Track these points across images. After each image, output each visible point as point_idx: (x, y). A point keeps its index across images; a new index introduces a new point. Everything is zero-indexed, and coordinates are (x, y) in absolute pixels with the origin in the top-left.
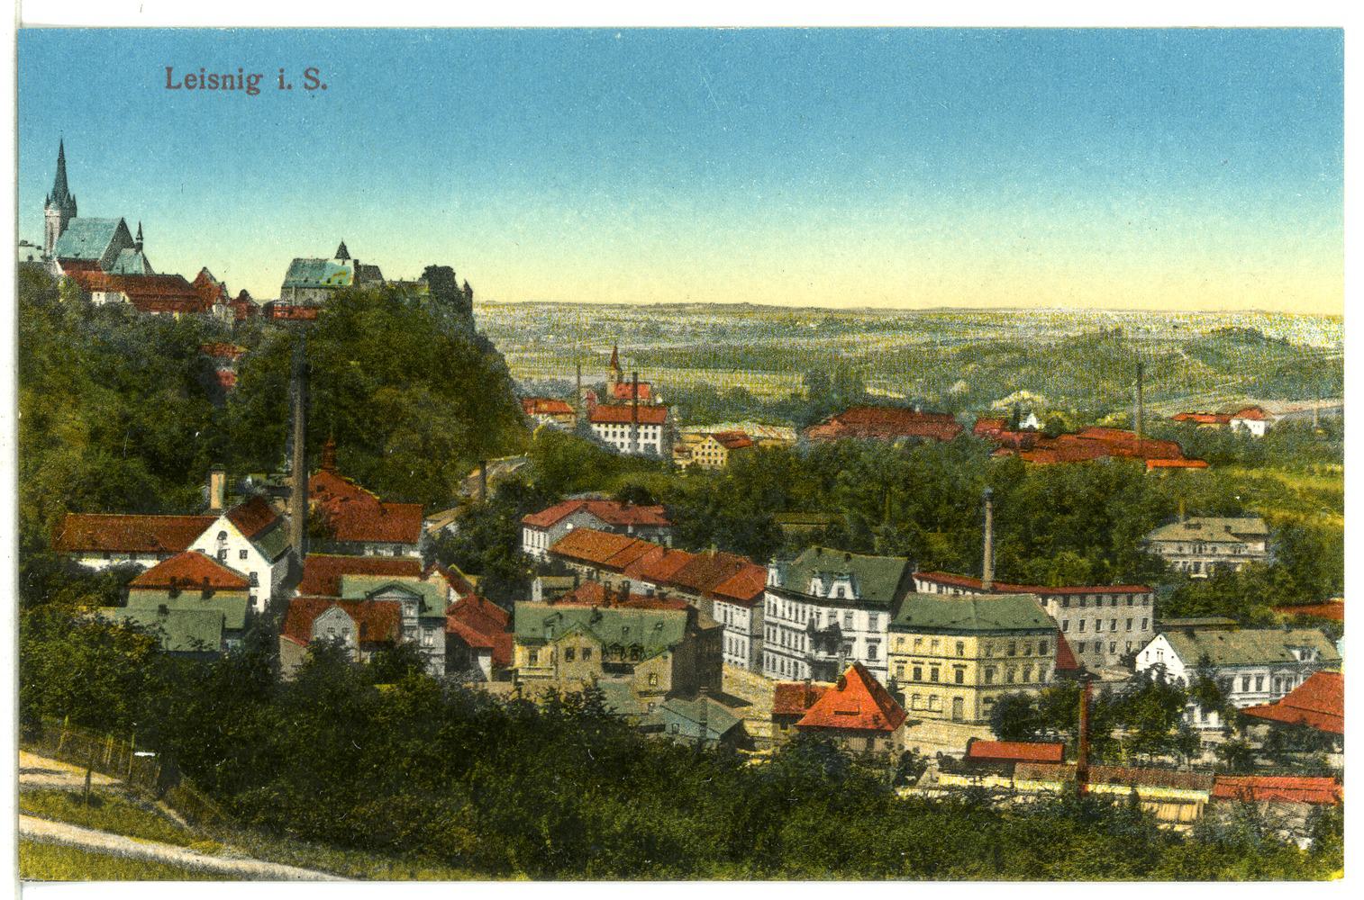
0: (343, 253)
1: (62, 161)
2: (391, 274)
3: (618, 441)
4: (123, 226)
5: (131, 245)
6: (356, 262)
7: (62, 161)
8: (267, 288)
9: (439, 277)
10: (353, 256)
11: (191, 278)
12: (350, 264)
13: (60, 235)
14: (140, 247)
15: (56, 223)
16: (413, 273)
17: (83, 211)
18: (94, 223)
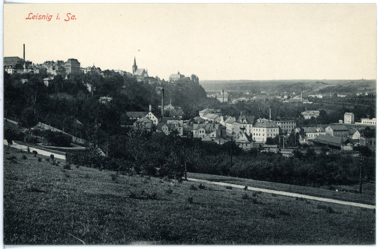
0: (179, 73)
1: (135, 61)
2: (186, 76)
3: (221, 100)
4: (144, 70)
5: (146, 73)
6: (181, 75)
7: (135, 61)
8: (167, 79)
9: (194, 76)
10: (180, 74)
11: (155, 77)
12: (180, 75)
13: (135, 71)
14: (147, 73)
15: (134, 70)
16: (190, 76)
17: (138, 68)
18: (140, 69)
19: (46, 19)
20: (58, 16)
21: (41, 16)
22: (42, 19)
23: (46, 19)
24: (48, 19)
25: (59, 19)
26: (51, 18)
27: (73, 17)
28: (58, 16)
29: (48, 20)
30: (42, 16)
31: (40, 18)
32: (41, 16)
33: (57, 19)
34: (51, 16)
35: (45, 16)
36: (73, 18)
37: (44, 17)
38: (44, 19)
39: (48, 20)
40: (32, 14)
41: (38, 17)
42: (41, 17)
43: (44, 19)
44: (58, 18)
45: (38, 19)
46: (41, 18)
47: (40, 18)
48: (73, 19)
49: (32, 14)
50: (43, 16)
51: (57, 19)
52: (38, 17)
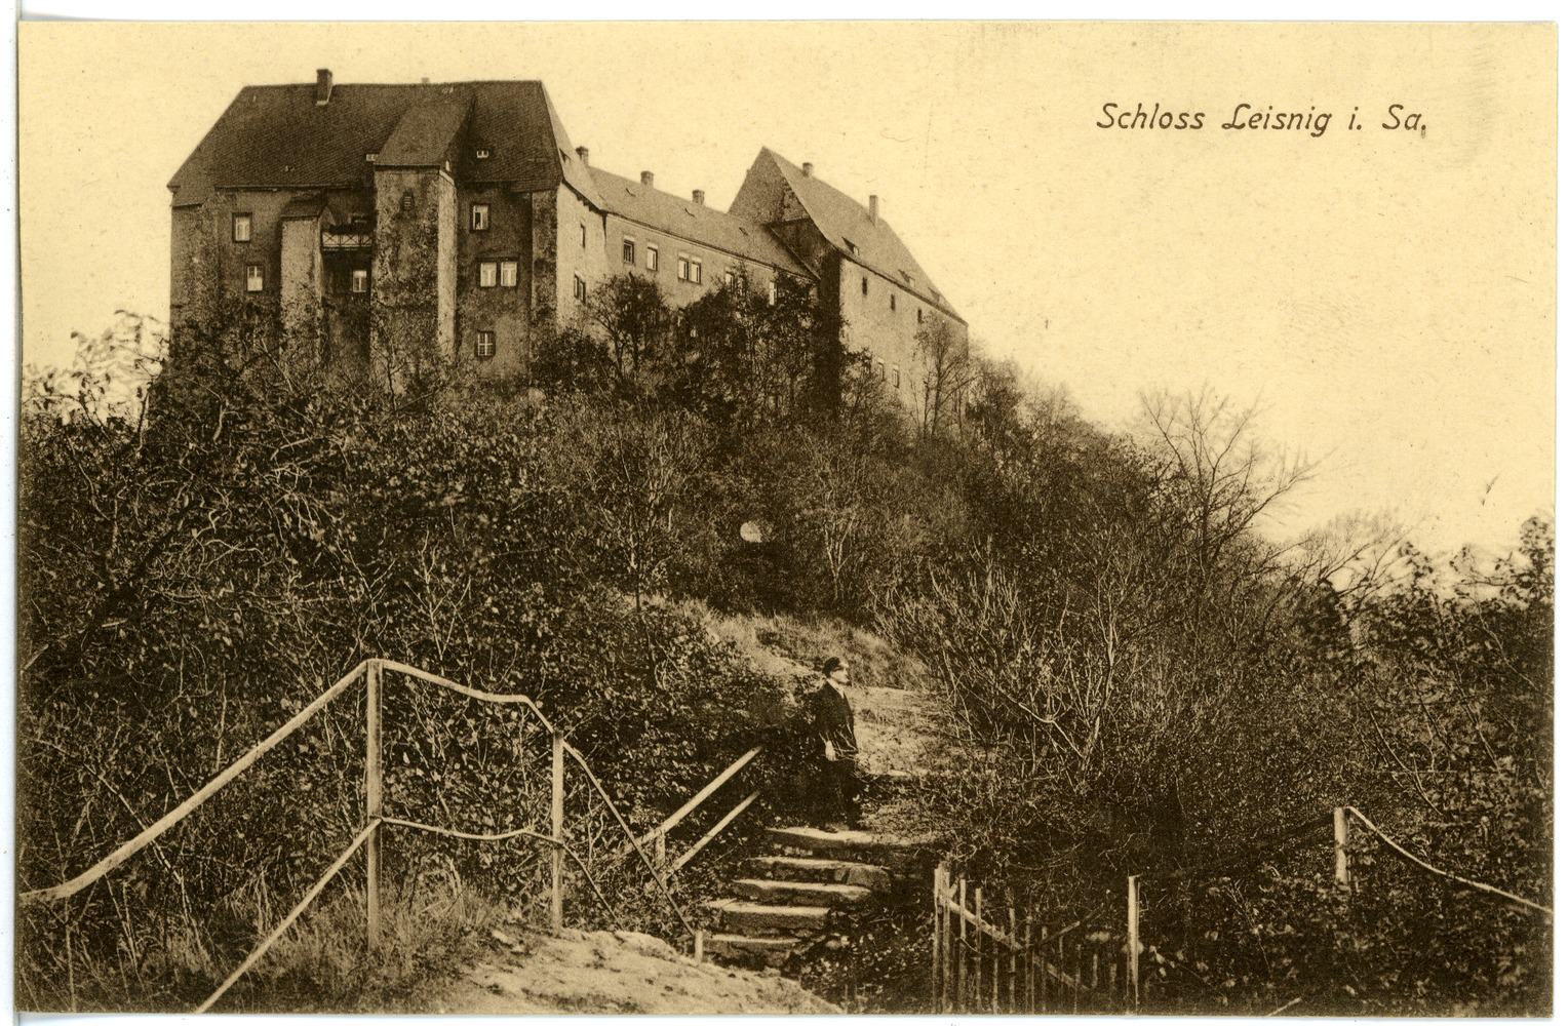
19: (1307, 127)
20: (1354, 116)
21: (1284, 115)
22: (1289, 127)
23: (1307, 127)
24: (1312, 129)
25: (1359, 127)
26: (1325, 127)
27: (1415, 123)
28: (1354, 116)
29: (1313, 135)
30: (1289, 117)
31: (1279, 125)
32: (1284, 115)
33: (1351, 128)
34: (1325, 115)
35: (1301, 116)
36: (1411, 122)
37: (1297, 119)
38: (1298, 127)
39: (1313, 135)
40: (1248, 106)
41: (1273, 121)
42: (1286, 121)
43: (1298, 127)
44: (1355, 126)
45: (1274, 127)
46: (1286, 123)
47: (1279, 125)
48: (1415, 127)
49: (1248, 106)
50: (1293, 116)
51: (1351, 128)
52: (1273, 121)
